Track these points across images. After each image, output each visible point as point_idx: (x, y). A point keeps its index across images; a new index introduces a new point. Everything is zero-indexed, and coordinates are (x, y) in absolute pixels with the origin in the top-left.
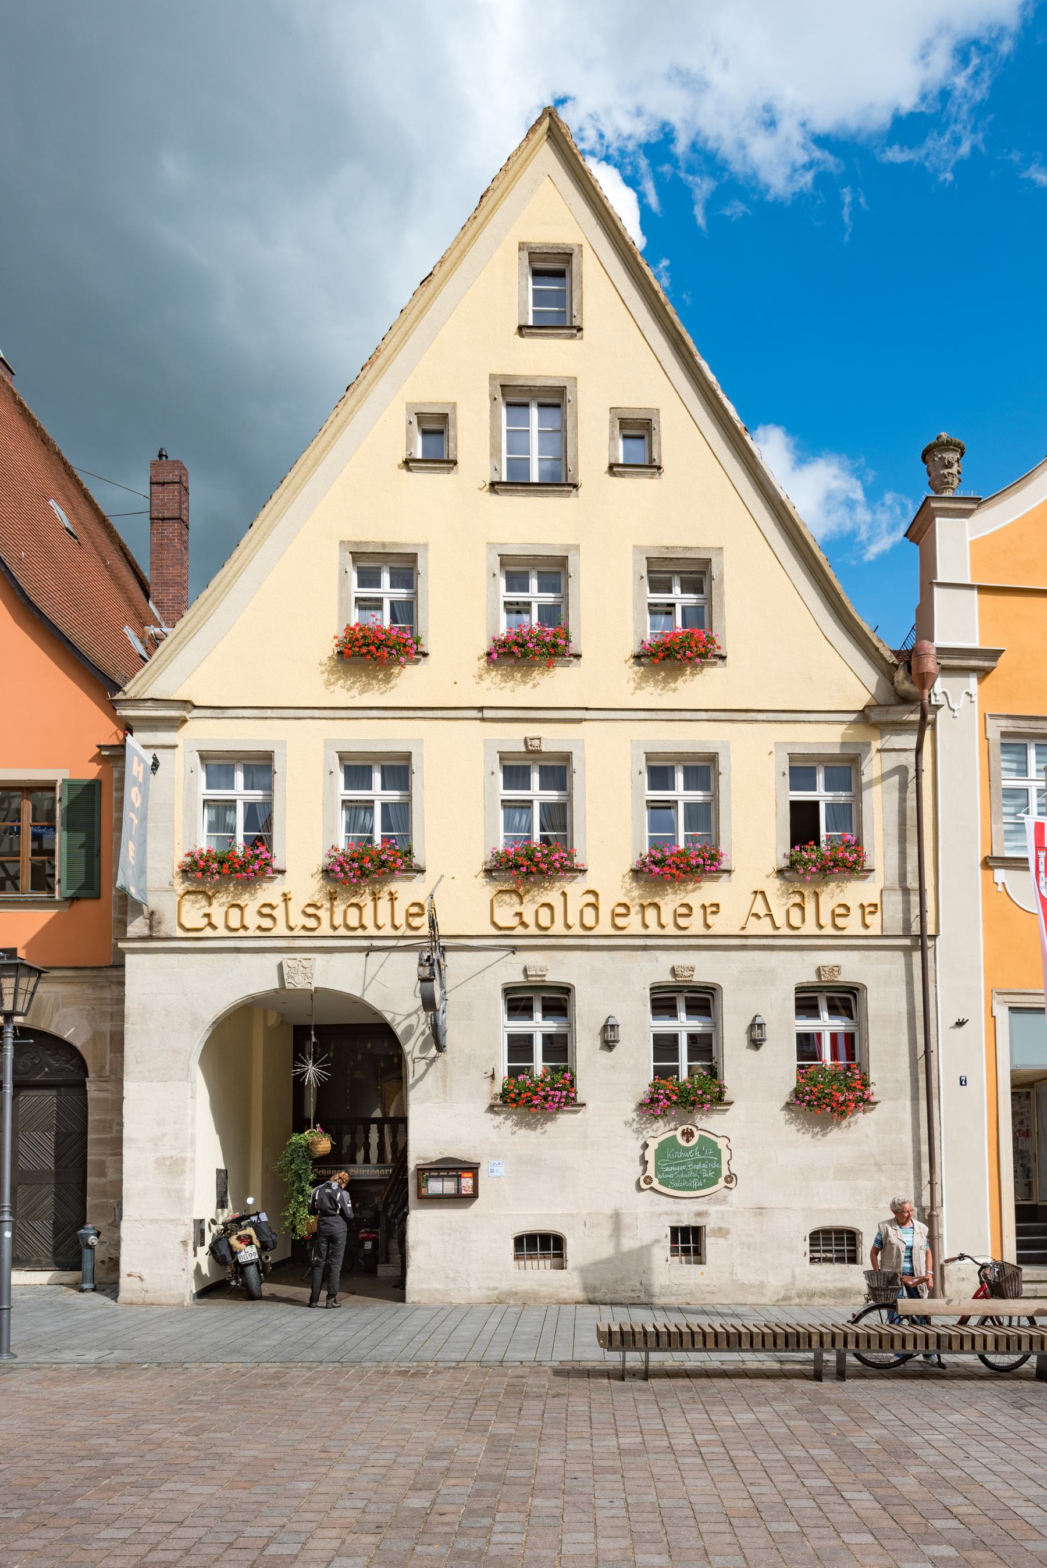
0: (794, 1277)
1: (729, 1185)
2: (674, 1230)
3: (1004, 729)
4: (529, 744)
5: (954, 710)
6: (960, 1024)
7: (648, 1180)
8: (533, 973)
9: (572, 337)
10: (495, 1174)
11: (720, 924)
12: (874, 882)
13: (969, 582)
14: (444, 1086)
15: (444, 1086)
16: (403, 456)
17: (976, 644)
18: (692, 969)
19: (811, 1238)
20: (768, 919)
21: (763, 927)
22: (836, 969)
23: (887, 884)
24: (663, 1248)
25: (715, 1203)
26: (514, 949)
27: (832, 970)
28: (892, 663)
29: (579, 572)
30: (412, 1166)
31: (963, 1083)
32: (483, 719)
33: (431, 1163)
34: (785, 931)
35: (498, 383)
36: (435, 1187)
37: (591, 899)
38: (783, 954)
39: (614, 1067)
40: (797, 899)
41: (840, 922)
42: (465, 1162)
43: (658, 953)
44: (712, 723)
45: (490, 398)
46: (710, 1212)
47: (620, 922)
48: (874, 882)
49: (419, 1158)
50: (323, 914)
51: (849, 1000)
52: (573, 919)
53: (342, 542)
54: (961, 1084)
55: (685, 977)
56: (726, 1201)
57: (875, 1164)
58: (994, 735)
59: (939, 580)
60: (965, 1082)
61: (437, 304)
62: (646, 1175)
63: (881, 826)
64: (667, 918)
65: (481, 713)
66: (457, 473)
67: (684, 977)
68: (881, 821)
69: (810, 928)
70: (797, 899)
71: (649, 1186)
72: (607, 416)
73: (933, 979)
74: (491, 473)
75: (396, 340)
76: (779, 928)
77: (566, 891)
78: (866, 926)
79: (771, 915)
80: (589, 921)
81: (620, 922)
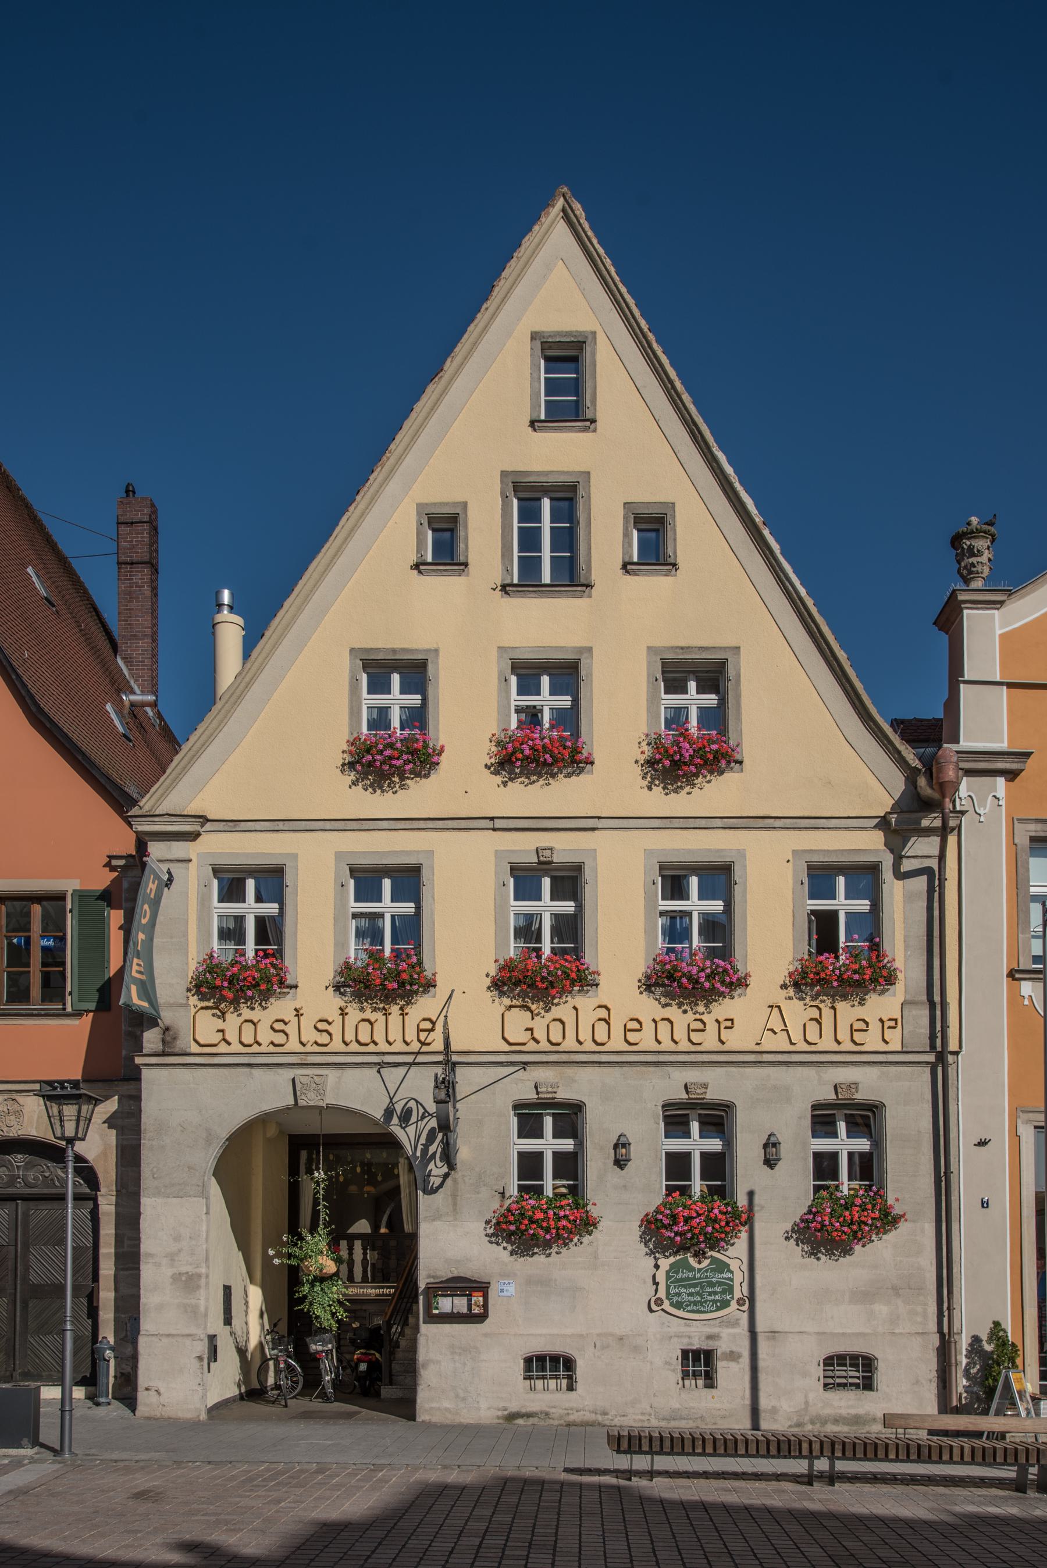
0: (807, 1403)
1: (740, 1308)
2: (685, 1353)
4: (540, 854)
5: (980, 815)
6: (982, 1143)
7: (659, 1302)
8: (544, 1090)
9: (586, 429)
10: (505, 1293)
11: (734, 1040)
12: (895, 996)
14: (455, 1204)
15: (455, 1204)
16: (413, 558)
18: (705, 1086)
19: (825, 1365)
20: (785, 1033)
21: (780, 1043)
22: (854, 1086)
23: (908, 997)
24: (674, 1371)
25: (727, 1327)
26: (525, 1065)
27: (849, 1087)
28: (915, 767)
29: (592, 675)
30: (422, 1286)
32: (494, 830)
33: (441, 1282)
34: (803, 1047)
35: (509, 480)
36: (445, 1304)
37: (603, 1013)
38: (800, 1069)
39: (625, 1186)
40: (815, 1014)
41: (857, 1036)
42: (475, 1281)
43: (670, 1069)
44: (727, 831)
45: (502, 497)
46: (722, 1335)
47: (632, 1037)
48: (895, 996)
49: (429, 1276)
50: (335, 1029)
51: (868, 1117)
52: (585, 1035)
53: (352, 650)
54: (983, 1206)
55: (698, 1094)
56: (738, 1324)
57: (892, 1288)
58: (1022, 840)
59: (966, 678)
61: (448, 399)
62: (657, 1296)
63: (902, 937)
64: (680, 1034)
65: (493, 823)
66: (468, 575)
67: (697, 1094)
68: (903, 932)
69: (827, 1043)
70: (815, 1014)
71: (660, 1308)
72: (621, 512)
73: (955, 1097)
74: (503, 574)
75: (406, 439)
76: (795, 1044)
77: (578, 1006)
79: (787, 1030)
80: (601, 1036)
81: (632, 1037)
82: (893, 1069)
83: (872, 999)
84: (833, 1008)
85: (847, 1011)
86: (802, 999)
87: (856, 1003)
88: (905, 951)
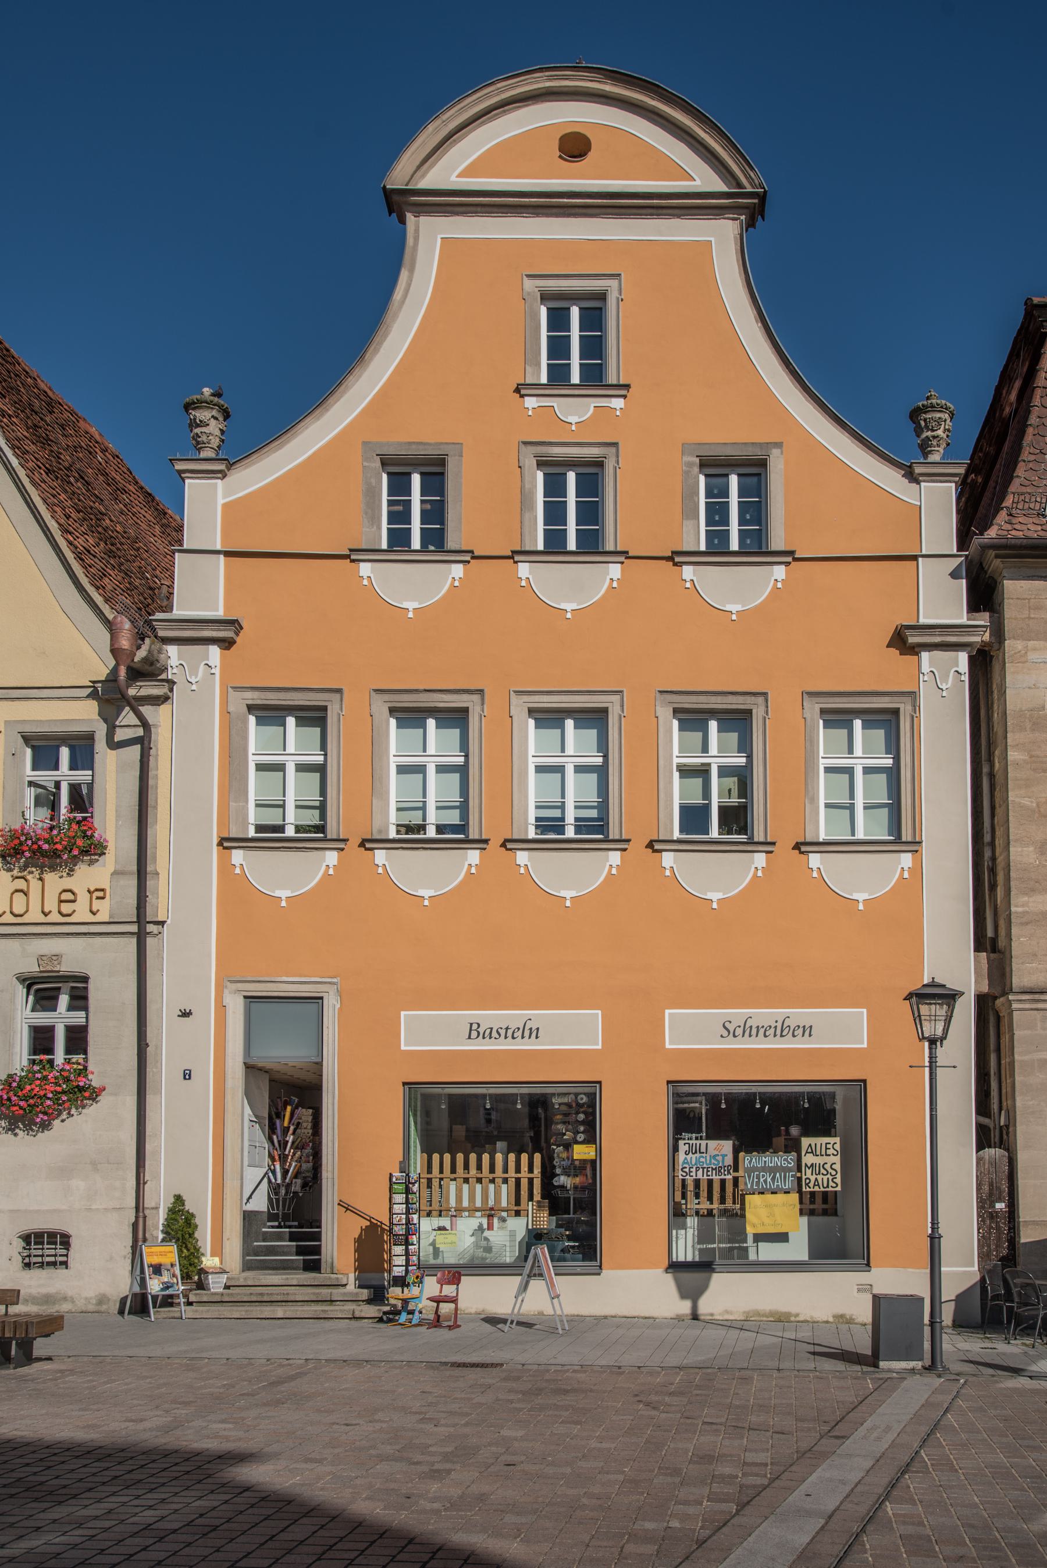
3: (250, 702)
12: (104, 866)
13: (219, 547)
17: (220, 613)
31: (187, 1077)
41: (66, 908)
48: (104, 866)
54: (185, 1078)
60: (190, 1075)
69: (35, 915)
78: (94, 914)
82: (98, 940)
83: (82, 869)
84: (41, 879)
85: (54, 881)
86: (10, 870)
87: (65, 874)
88: (117, 820)
